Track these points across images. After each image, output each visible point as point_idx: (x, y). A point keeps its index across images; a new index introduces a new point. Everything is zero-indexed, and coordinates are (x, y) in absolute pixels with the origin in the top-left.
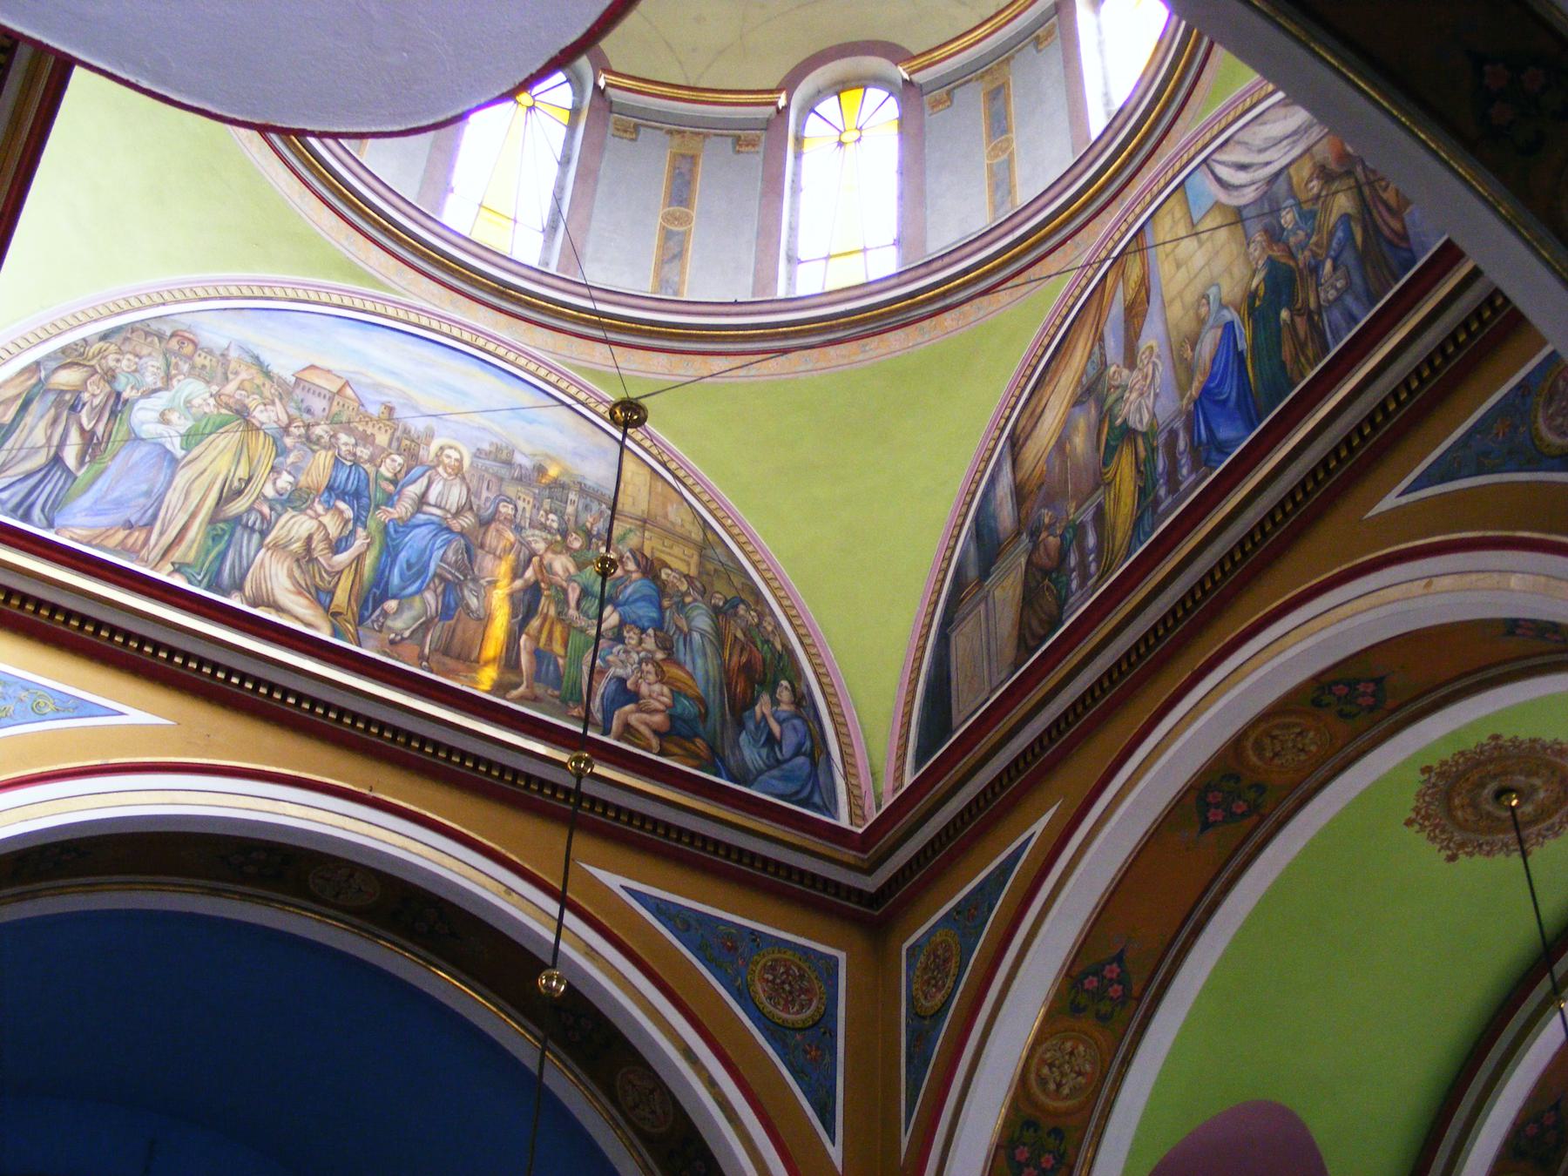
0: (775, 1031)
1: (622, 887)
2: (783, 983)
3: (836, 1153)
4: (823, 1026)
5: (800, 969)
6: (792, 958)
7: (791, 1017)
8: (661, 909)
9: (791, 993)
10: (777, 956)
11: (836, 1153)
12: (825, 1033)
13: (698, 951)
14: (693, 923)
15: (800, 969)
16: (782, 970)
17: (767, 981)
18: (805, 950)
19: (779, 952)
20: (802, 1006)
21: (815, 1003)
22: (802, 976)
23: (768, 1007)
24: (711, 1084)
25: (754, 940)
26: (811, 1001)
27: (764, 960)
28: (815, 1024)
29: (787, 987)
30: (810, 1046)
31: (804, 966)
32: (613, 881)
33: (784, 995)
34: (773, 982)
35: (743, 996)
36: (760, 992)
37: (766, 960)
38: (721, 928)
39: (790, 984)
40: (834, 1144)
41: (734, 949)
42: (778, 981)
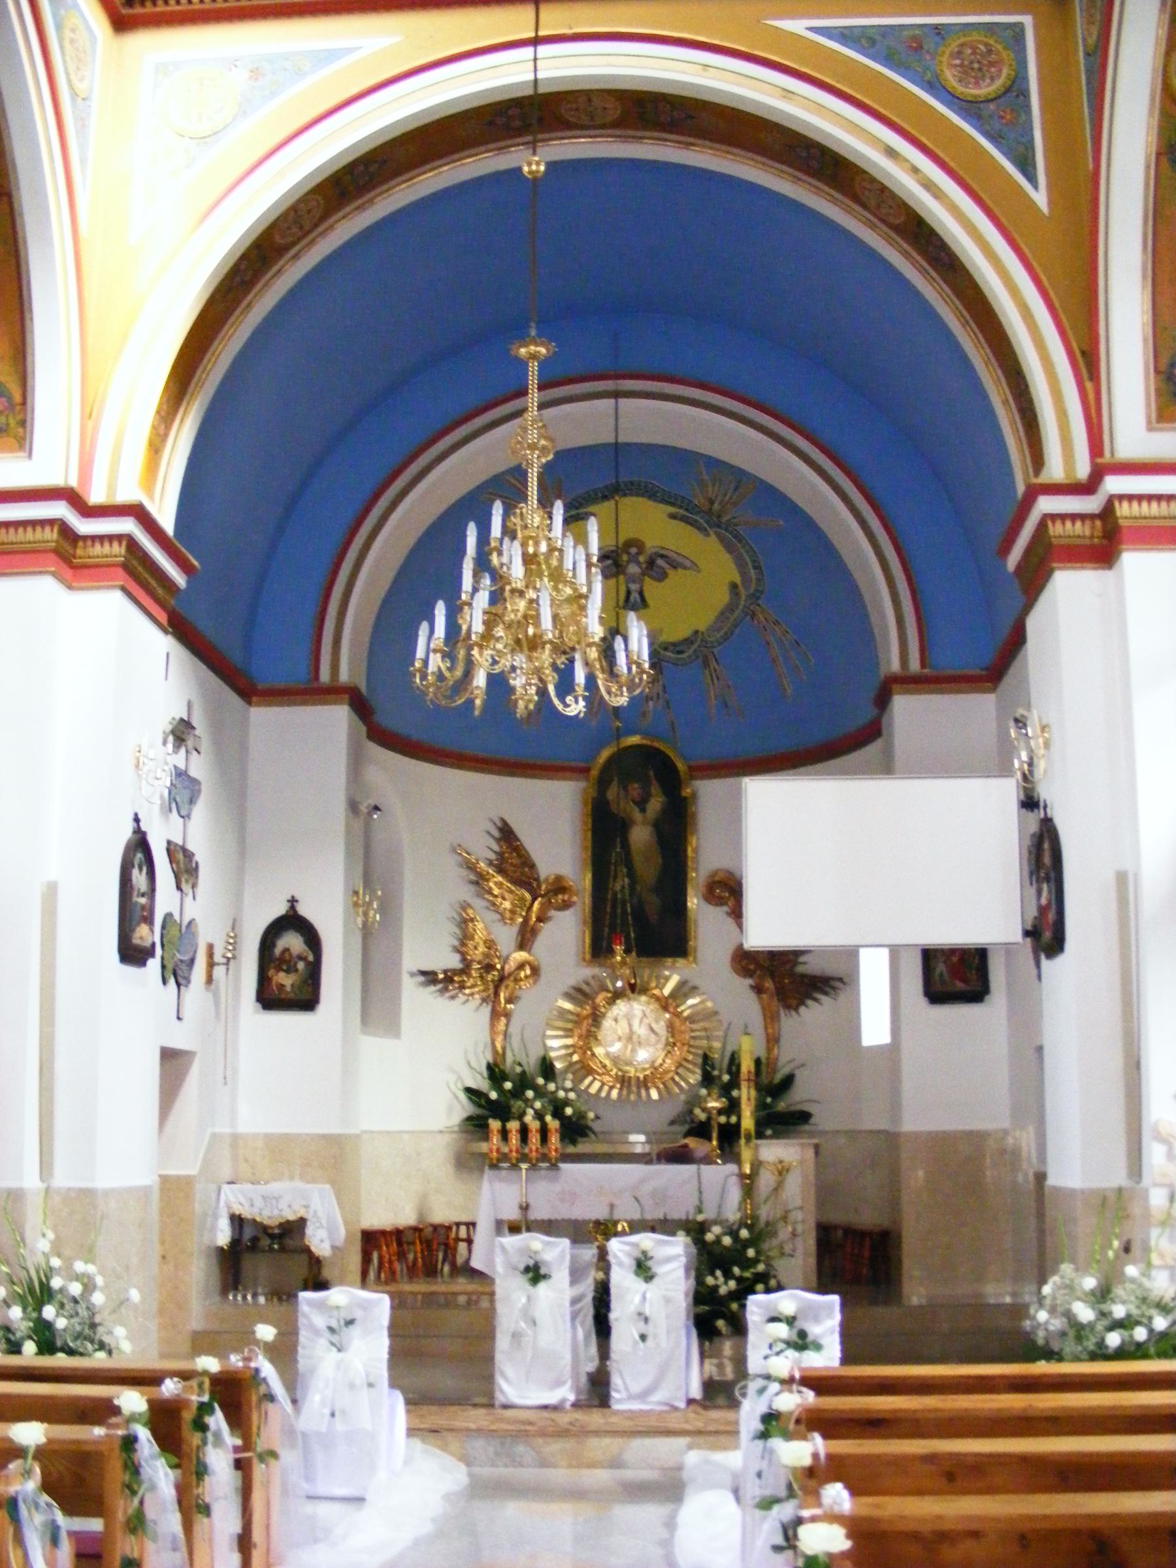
0: (970, 108)
1: (807, 29)
2: (971, 63)
3: (1040, 198)
4: (1016, 90)
5: (986, 45)
6: (978, 38)
7: (986, 89)
8: (845, 36)
9: (980, 69)
10: (963, 40)
11: (1040, 198)
12: (1017, 96)
13: (889, 60)
14: (878, 38)
15: (986, 45)
16: (969, 51)
17: (956, 66)
18: (990, 28)
19: (964, 36)
20: (992, 79)
21: (1005, 71)
22: (990, 52)
23: (960, 89)
24: (915, 170)
25: (939, 34)
26: (1000, 71)
27: (950, 49)
28: (1008, 90)
29: (976, 66)
30: (1003, 111)
31: (991, 42)
32: (797, 26)
33: (973, 74)
34: (961, 65)
35: (934, 86)
36: (950, 77)
37: (954, 46)
38: (905, 33)
39: (979, 62)
40: (1036, 187)
41: (921, 47)
42: (966, 63)
